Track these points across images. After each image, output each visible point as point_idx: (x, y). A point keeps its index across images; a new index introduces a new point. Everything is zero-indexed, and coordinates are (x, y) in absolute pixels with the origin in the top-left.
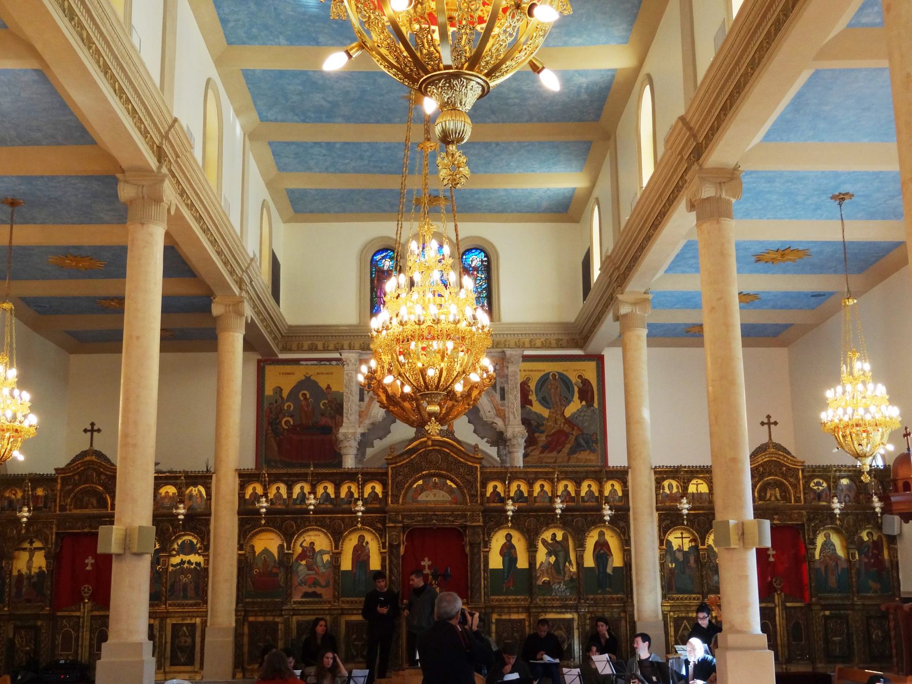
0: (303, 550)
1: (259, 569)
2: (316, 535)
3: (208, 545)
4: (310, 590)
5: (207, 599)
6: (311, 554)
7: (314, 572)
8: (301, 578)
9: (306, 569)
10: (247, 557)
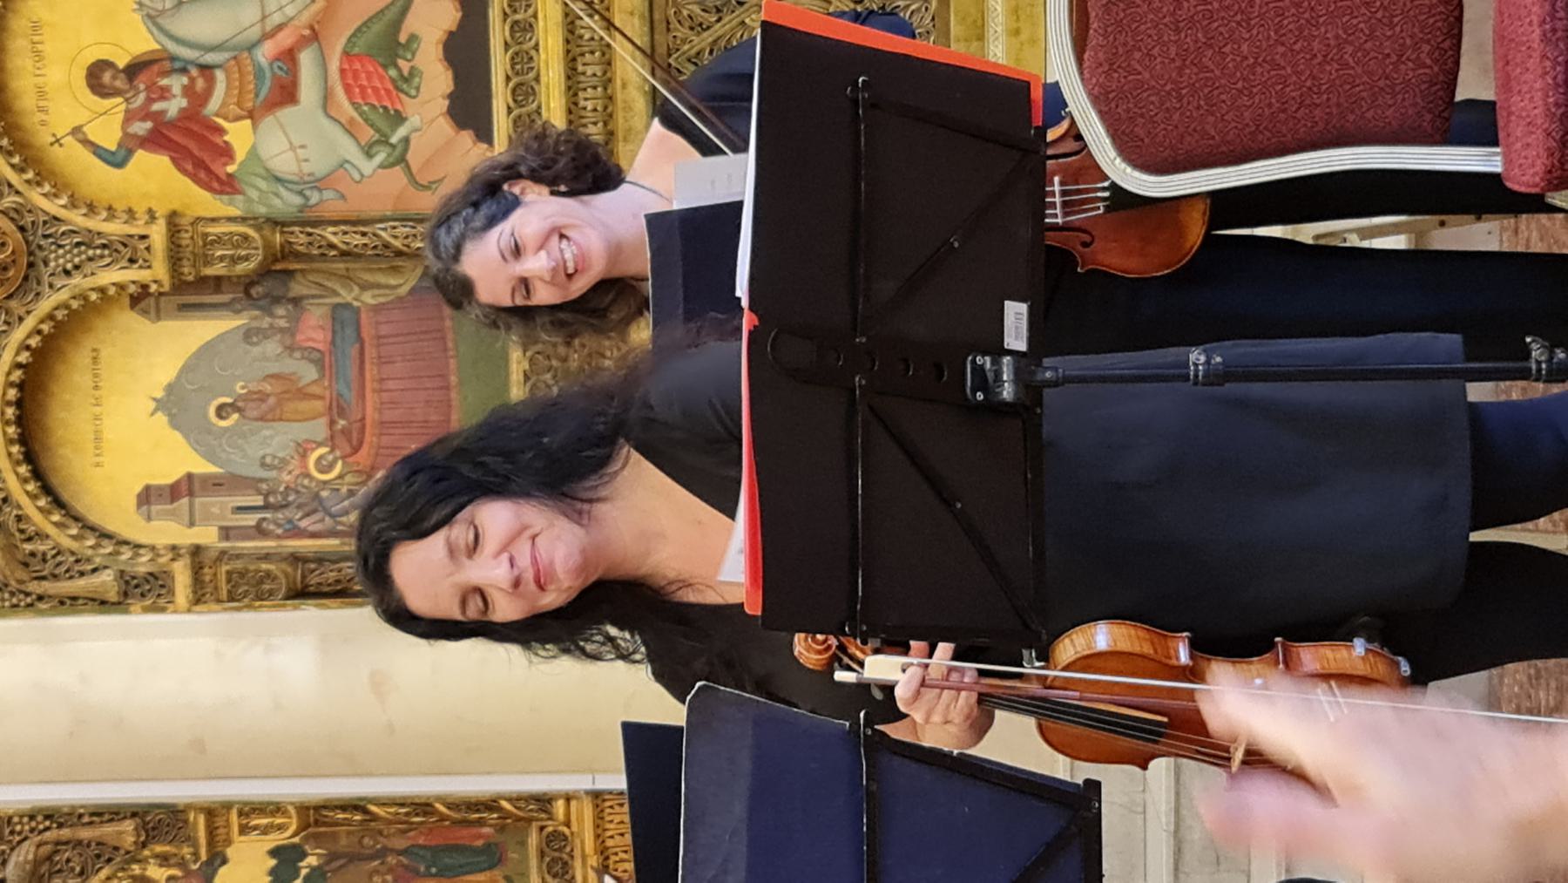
0: (158, 139)
1: (303, 451)
2: (39, 55)
3: (136, 812)
4: (437, 79)
5: (515, 799)
6: (176, 83)
7: (306, 59)
8: (350, 150)
9: (286, 113)
10: (226, 533)
